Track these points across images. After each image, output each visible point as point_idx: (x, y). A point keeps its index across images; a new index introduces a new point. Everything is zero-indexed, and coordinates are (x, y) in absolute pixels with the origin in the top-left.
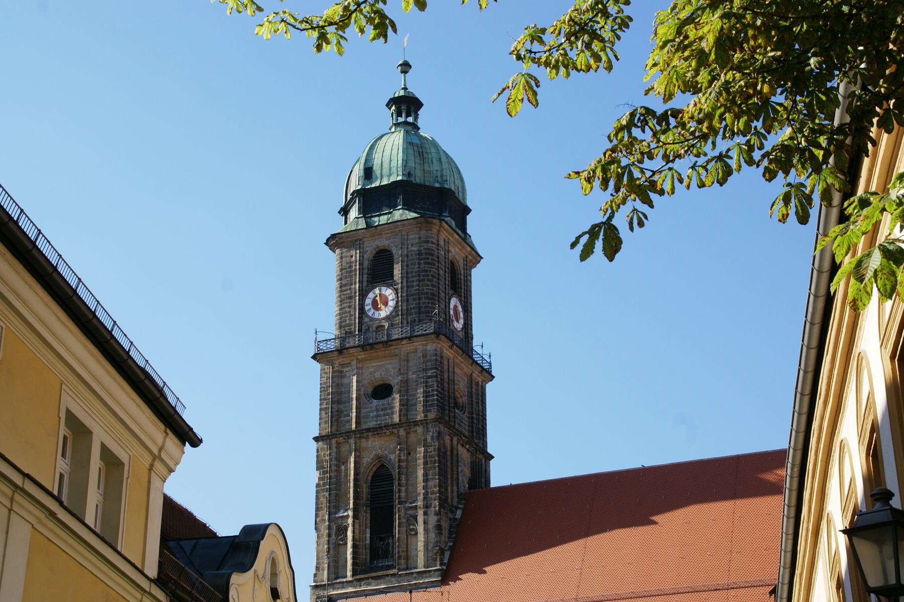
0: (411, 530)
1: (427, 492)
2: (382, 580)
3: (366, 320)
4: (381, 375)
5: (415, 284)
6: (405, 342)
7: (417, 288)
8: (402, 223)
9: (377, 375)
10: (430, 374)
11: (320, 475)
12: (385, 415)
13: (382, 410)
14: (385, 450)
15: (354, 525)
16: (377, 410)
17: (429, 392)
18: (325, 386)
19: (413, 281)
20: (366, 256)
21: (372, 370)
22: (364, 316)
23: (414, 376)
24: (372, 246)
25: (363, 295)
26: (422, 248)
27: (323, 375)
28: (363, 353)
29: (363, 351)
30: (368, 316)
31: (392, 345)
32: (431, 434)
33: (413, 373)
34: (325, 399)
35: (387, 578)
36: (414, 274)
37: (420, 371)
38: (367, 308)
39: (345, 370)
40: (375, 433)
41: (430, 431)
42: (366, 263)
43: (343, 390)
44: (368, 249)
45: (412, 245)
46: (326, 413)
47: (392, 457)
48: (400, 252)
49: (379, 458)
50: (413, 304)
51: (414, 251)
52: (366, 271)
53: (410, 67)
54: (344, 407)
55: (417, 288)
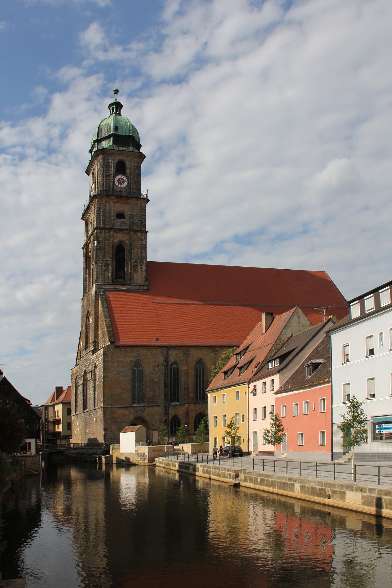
0: (136, 270)
1: (142, 258)
2: (125, 286)
3: (115, 187)
4: (122, 209)
5: (136, 178)
6: (135, 199)
7: (136, 180)
8: (133, 153)
9: (120, 209)
10: (143, 214)
11: (97, 242)
12: (124, 225)
13: (122, 223)
14: (124, 238)
15: (112, 264)
16: (120, 223)
17: (143, 221)
18: (99, 208)
19: (135, 177)
20: (115, 161)
21: (118, 207)
22: (114, 185)
23: (136, 213)
24: (117, 158)
25: (114, 177)
26: (138, 165)
27: (98, 204)
28: (116, 199)
29: (117, 198)
30: (116, 185)
31: (129, 199)
32: (144, 236)
33: (135, 212)
34: (99, 213)
35: (127, 286)
36: (135, 174)
37: (139, 212)
38: (115, 182)
39: (107, 204)
40: (121, 231)
41: (143, 235)
42: (115, 164)
43: (106, 212)
44: (116, 159)
45: (135, 163)
46: (100, 219)
47: (127, 242)
48: (130, 164)
49: (121, 241)
50: (135, 186)
51: (136, 165)
52: (115, 167)
53: (118, 91)
54: (106, 218)
55: (136, 180)
